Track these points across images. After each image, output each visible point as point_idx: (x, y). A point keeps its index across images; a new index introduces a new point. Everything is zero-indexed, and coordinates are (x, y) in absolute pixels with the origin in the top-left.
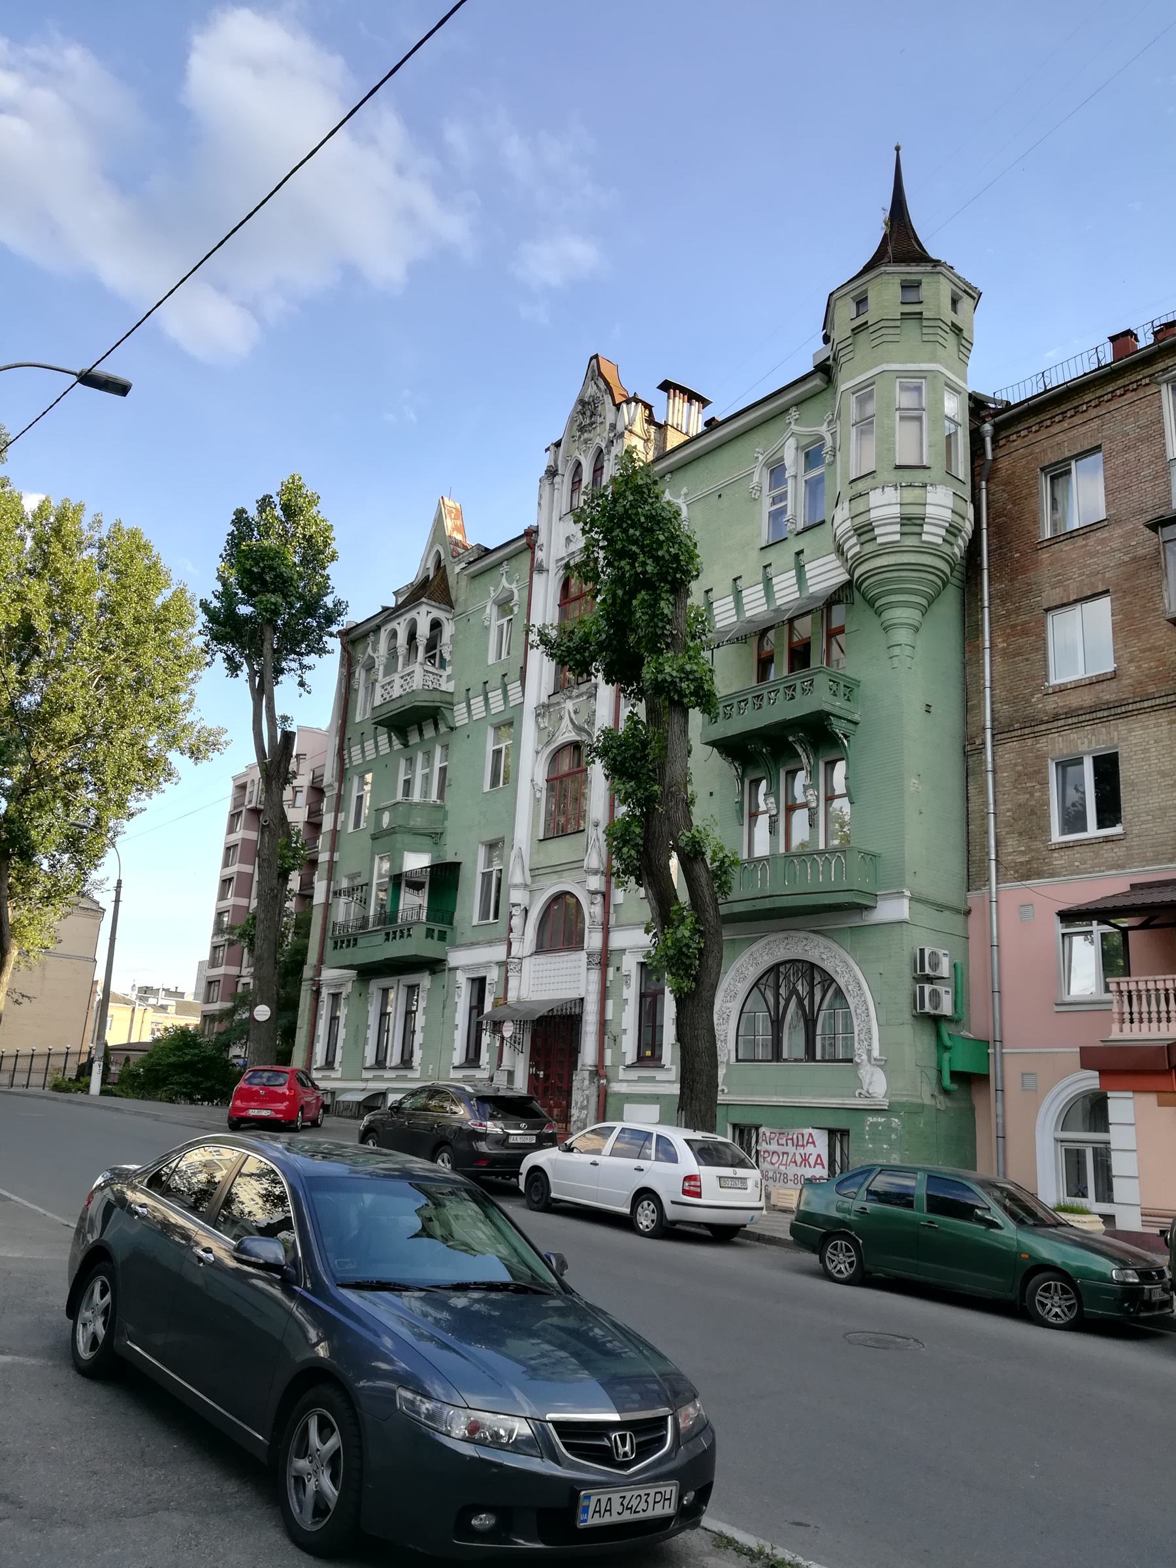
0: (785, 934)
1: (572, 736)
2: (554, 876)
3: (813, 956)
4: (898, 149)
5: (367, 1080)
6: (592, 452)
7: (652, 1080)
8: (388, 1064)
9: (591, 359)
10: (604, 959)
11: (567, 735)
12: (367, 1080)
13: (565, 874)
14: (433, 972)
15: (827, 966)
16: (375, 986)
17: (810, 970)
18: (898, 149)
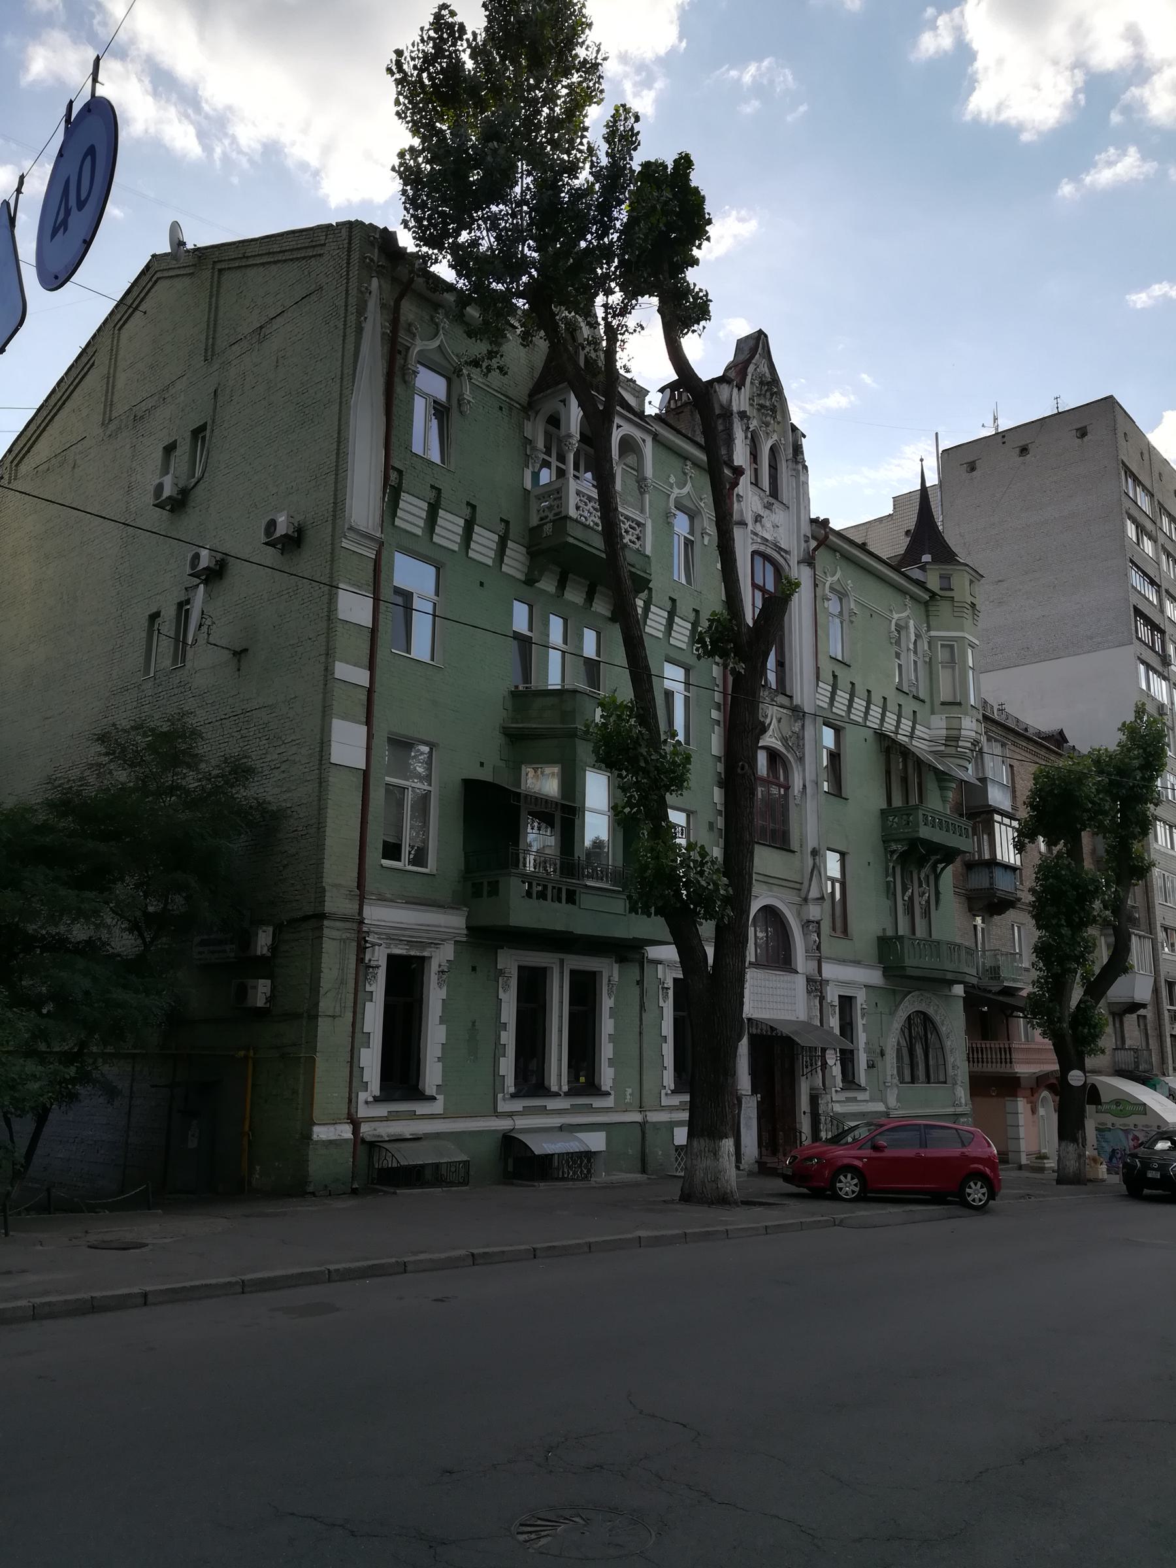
0: (917, 993)
1: (778, 745)
2: (765, 887)
3: (930, 1011)
4: (922, 460)
5: (511, 1115)
6: (770, 443)
7: (855, 1100)
8: (554, 1088)
9: (760, 332)
10: (816, 986)
11: (773, 740)
12: (511, 1115)
13: (775, 888)
14: (621, 960)
15: (937, 1019)
16: (510, 962)
17: (926, 1019)
18: (922, 460)
